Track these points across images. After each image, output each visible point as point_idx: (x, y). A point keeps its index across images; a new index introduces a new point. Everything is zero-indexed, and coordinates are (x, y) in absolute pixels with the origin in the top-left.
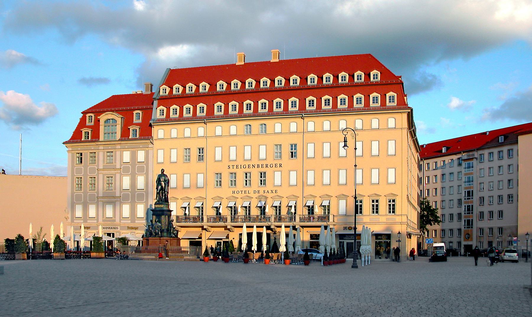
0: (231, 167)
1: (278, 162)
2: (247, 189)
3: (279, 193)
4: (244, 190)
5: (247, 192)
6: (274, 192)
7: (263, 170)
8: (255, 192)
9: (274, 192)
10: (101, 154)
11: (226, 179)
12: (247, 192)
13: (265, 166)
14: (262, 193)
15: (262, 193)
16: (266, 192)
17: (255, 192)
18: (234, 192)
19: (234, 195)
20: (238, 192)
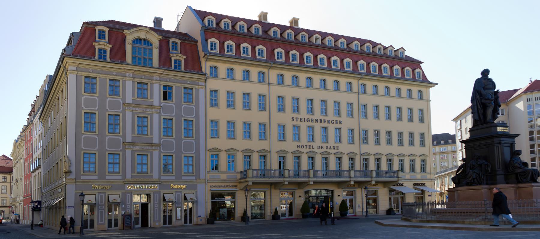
0: (295, 119)
1: (338, 119)
6: (336, 148)
7: (326, 125)
9: (336, 148)
10: (129, 84)
11: (289, 132)
14: (325, 149)
15: (325, 148)
18: (298, 147)
19: (298, 149)
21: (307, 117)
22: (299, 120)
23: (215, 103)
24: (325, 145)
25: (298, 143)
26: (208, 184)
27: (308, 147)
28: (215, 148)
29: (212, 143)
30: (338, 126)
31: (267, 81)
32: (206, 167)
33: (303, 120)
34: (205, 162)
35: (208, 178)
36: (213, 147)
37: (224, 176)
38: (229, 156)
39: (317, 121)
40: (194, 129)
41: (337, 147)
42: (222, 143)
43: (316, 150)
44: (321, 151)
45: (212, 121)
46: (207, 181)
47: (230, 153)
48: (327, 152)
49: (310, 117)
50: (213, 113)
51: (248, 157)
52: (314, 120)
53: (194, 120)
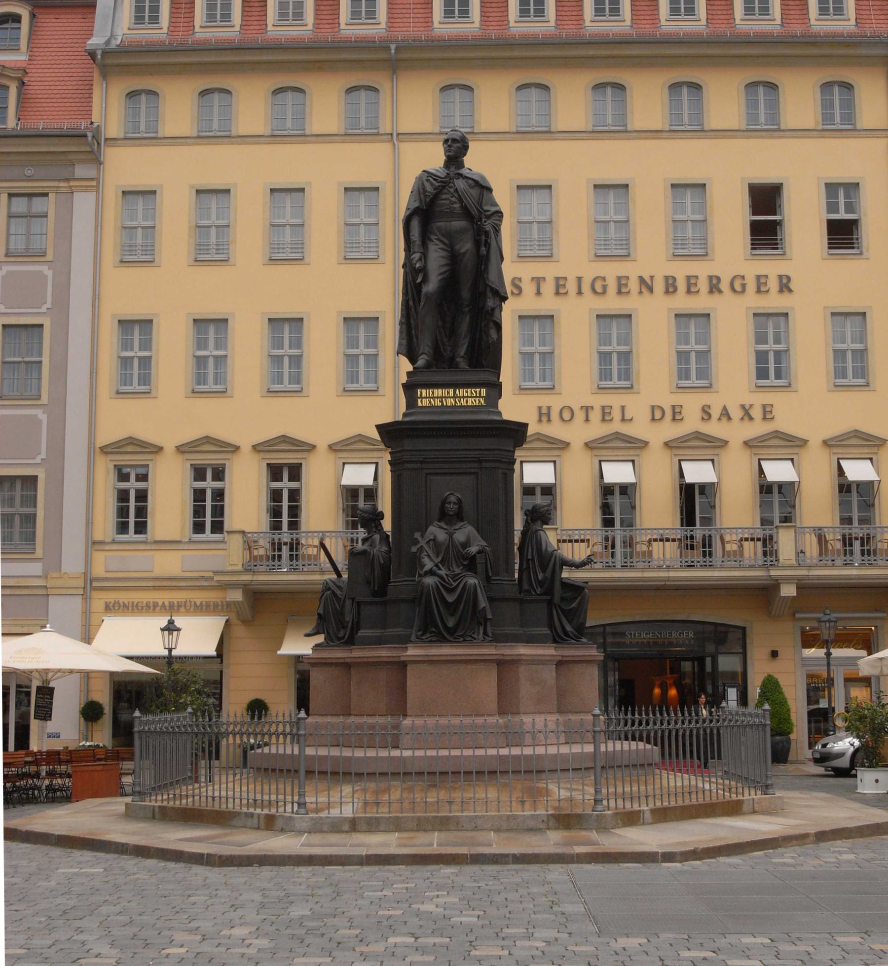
0: (528, 288)
2: (615, 401)
3: (785, 422)
4: (599, 401)
5: (616, 414)
6: (757, 413)
7: (700, 302)
8: (656, 414)
9: (757, 413)
12: (616, 414)
13: (703, 285)
14: (692, 423)
16: (716, 412)
17: (656, 414)
20: (567, 415)
21: (590, 271)
22: (548, 288)
23: (139, 251)
24: (692, 403)
25: (545, 400)
26: (96, 595)
27: (596, 415)
28: (131, 441)
29: (121, 419)
30: (774, 302)
31: (385, 126)
32: (89, 523)
33: (572, 286)
34: (81, 501)
35: (99, 570)
36: (125, 435)
37: (169, 563)
38: (199, 473)
39: (646, 285)
40: (46, 360)
41: (767, 413)
42: (169, 417)
43: (639, 429)
44: (670, 431)
45: (126, 325)
46: (91, 585)
47: (201, 459)
48: (697, 436)
49: (611, 271)
50: (129, 292)
51: (284, 472)
52: (634, 285)
53: (46, 322)
